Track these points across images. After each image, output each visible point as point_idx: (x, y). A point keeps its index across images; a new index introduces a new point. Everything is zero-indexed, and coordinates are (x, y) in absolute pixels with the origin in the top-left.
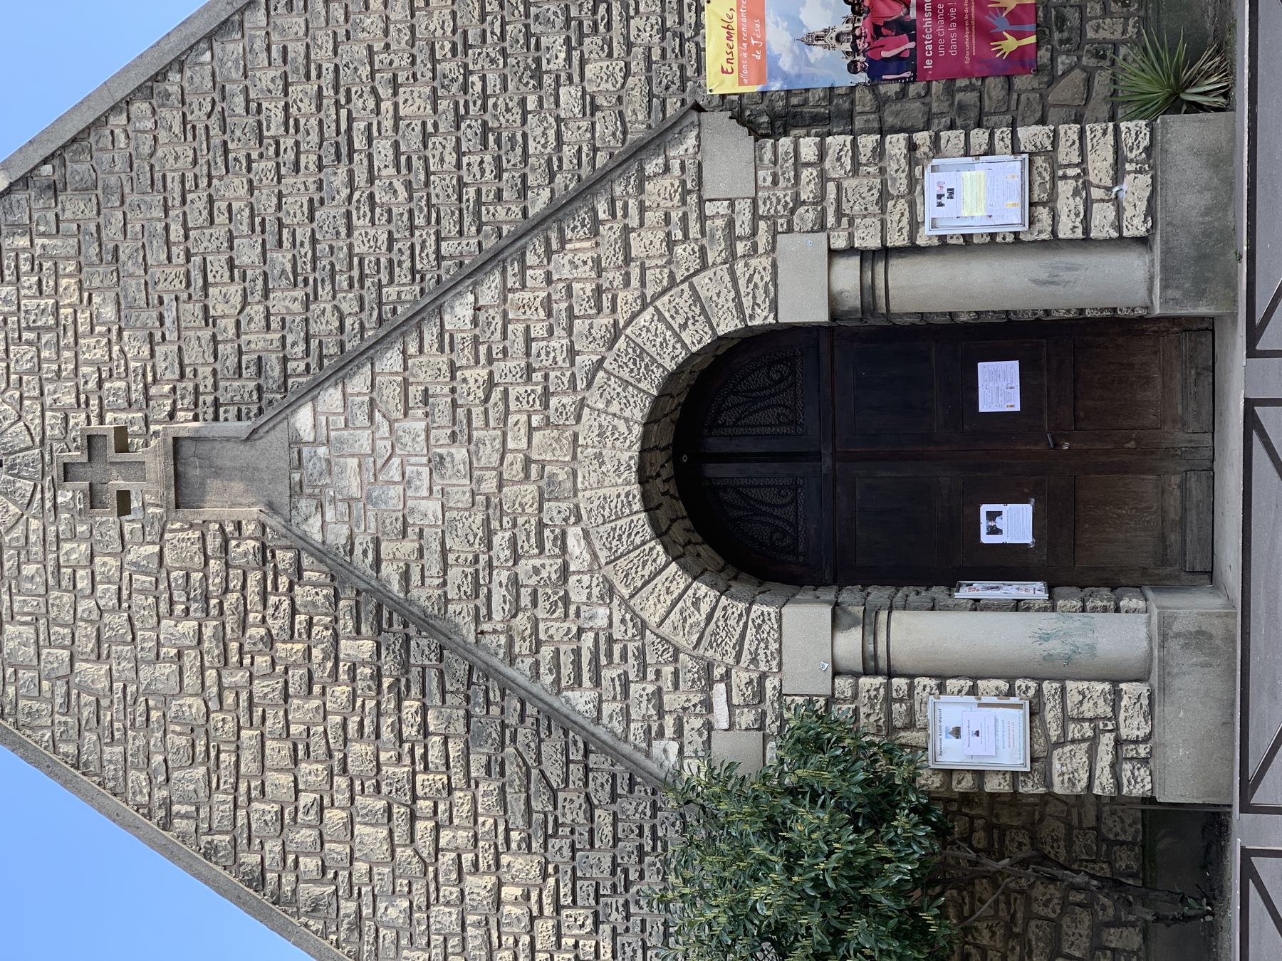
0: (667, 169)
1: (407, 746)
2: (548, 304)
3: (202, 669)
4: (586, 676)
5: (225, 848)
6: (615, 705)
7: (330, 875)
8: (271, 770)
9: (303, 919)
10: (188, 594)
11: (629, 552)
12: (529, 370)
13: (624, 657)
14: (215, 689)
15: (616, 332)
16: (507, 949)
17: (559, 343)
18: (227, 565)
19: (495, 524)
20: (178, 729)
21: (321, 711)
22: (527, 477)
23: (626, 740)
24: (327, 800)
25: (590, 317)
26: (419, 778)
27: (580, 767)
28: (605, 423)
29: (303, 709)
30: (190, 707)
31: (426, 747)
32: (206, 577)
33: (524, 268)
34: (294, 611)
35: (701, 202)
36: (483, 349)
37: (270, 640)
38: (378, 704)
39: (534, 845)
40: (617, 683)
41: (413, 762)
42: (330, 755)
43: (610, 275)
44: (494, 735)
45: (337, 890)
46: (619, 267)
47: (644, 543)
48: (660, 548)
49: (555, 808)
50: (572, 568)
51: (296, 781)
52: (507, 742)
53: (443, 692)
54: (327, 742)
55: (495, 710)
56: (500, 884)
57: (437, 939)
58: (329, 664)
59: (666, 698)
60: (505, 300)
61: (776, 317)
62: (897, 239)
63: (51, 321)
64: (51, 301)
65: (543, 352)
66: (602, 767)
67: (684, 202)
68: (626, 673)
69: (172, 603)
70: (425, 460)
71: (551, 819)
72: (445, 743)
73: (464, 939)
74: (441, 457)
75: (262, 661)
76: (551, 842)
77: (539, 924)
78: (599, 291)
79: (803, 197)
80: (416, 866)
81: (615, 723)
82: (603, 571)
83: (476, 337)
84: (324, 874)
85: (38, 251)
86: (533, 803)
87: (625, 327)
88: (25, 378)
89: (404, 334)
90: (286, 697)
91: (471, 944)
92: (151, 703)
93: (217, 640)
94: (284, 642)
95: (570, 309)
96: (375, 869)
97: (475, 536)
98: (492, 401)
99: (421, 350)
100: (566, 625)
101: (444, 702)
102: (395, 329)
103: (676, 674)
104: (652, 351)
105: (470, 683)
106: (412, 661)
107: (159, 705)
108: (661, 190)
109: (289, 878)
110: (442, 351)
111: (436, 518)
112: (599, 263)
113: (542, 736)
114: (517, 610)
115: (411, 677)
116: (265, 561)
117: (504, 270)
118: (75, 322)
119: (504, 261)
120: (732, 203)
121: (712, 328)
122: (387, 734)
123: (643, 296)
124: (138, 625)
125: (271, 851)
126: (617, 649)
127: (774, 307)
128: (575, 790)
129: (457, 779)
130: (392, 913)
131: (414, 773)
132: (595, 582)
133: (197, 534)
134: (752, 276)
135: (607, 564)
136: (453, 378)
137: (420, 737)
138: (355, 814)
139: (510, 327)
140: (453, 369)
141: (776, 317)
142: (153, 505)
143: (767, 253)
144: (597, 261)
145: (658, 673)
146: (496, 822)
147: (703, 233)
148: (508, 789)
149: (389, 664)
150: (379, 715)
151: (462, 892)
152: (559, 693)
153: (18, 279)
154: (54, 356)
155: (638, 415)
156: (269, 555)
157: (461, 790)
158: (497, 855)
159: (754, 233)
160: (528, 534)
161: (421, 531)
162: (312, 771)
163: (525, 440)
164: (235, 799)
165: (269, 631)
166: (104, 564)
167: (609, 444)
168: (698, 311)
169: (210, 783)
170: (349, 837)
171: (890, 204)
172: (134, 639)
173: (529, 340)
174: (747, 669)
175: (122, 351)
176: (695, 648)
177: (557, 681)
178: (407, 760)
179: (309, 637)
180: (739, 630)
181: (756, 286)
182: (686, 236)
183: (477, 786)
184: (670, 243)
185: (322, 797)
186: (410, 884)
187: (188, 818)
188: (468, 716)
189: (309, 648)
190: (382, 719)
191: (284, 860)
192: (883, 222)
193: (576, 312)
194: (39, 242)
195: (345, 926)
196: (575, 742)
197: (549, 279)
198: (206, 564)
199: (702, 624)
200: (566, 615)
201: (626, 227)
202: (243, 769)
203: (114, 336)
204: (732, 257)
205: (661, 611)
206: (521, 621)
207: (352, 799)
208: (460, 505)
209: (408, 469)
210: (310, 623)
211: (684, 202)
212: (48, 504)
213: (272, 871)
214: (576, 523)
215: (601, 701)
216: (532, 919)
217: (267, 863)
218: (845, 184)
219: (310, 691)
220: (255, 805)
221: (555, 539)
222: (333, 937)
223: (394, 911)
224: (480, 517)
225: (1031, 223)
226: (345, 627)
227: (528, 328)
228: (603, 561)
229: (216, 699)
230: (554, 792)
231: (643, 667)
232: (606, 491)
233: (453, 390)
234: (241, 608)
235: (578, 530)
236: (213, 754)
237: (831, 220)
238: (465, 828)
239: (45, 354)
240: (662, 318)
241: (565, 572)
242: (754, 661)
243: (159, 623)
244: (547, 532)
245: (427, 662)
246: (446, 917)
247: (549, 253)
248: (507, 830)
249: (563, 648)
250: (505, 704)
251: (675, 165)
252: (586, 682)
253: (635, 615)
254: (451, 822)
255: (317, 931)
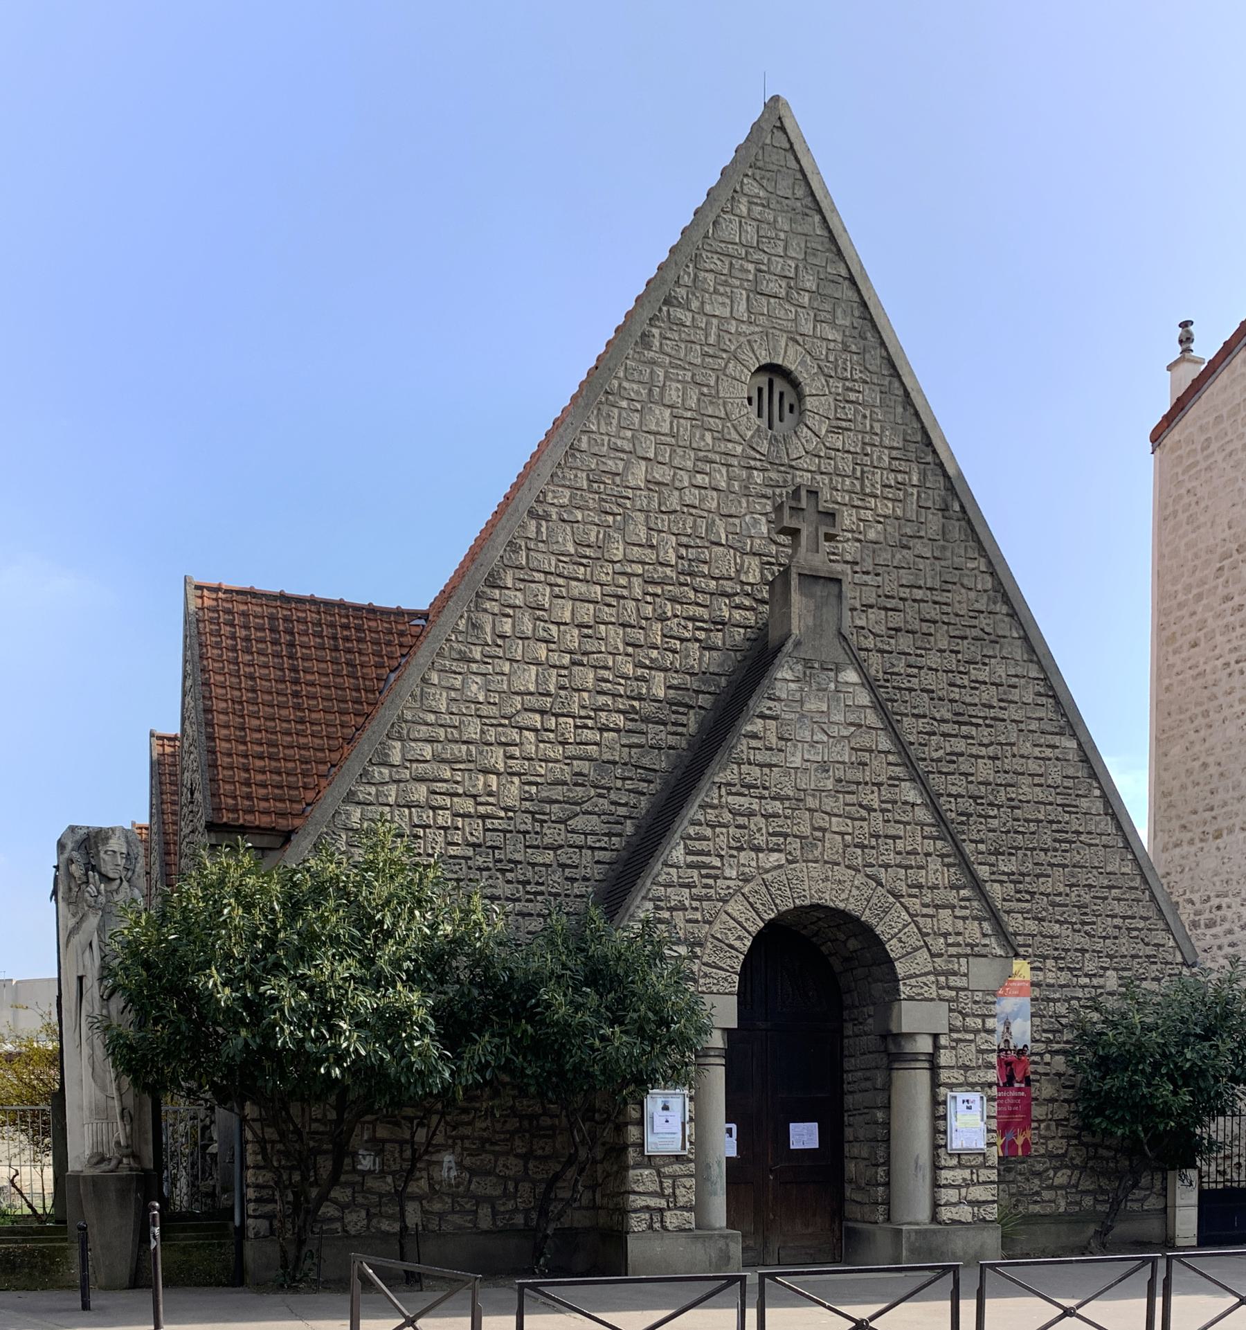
0: (985, 935)
1: (592, 714)
2: (914, 853)
3: (643, 563)
4: (695, 858)
5: (517, 559)
6: (675, 877)
7: (500, 642)
8: (573, 605)
9: (466, 615)
10: (693, 561)
11: (770, 895)
12: (877, 837)
13: (707, 886)
14: (629, 570)
15: (897, 896)
16: (452, 775)
17: (891, 858)
18: (712, 594)
19: (787, 804)
20: (601, 536)
21: (615, 651)
22: (815, 829)
23: (653, 883)
24: (553, 646)
25: (907, 879)
26: (570, 721)
27: (583, 843)
28: (846, 884)
29: (615, 636)
30: (617, 549)
31: (592, 728)
32: (704, 576)
33: (935, 838)
34: (682, 640)
35: (966, 956)
36: (889, 806)
37: (662, 619)
38: (621, 696)
39: (527, 803)
40: (691, 880)
41: (581, 717)
42: (585, 654)
43: (929, 895)
44: (603, 781)
45: (488, 645)
46: (933, 901)
47: (776, 905)
48: (773, 916)
49: (553, 822)
50: (761, 855)
51: (565, 624)
52: (598, 791)
53: (630, 746)
54: (594, 653)
55: (619, 783)
56: (498, 774)
57: (456, 720)
58: (647, 662)
59: (681, 913)
60: (916, 824)
61: (905, 999)
62: (944, 1076)
63: (868, 491)
64: (879, 492)
65: (887, 847)
66: (583, 859)
67: (967, 945)
68: (695, 887)
69: (687, 547)
70: (826, 759)
71: (546, 817)
72: (595, 744)
73: (457, 742)
74: (828, 771)
75: (648, 611)
76: (529, 816)
77: (471, 801)
78: (920, 887)
79: (967, 1019)
80: (509, 711)
81: (664, 877)
82: (758, 876)
83: (896, 802)
84: (499, 636)
85: (910, 490)
86: (556, 805)
87: (900, 902)
88: (832, 462)
89: (899, 753)
90: (624, 625)
91: (455, 747)
92: (619, 518)
93: (663, 578)
94: (662, 630)
95: (911, 867)
96: (505, 678)
97: (781, 789)
98: (860, 810)
99: (889, 764)
100: (725, 847)
101: (623, 746)
102: (903, 747)
103: (697, 921)
104: (887, 919)
105: (637, 767)
106: (650, 725)
107: (617, 524)
108: (973, 931)
109: (494, 607)
110: (889, 779)
111: (791, 763)
112: (935, 888)
113: (603, 817)
114: (734, 813)
115: (639, 723)
116: (715, 623)
117: (933, 826)
118: (867, 509)
119: (938, 826)
120: (966, 975)
121: (899, 958)
122: (601, 700)
123: (917, 915)
124: (672, 517)
125: (515, 596)
126: (711, 881)
127: (910, 999)
128: (566, 837)
129: (571, 751)
130: (474, 688)
131: (574, 717)
132: (752, 870)
133: (733, 575)
134: (927, 985)
135: (763, 879)
136: (874, 784)
137: (599, 725)
138: (543, 667)
139: (902, 826)
140: (879, 785)
141: (905, 999)
142: (752, 544)
143: (938, 995)
144: (936, 887)
145: (696, 909)
146: (542, 776)
147: (950, 956)
148: (565, 787)
149: (648, 708)
150: (614, 695)
151: (491, 744)
152: (682, 838)
153: (893, 471)
154: (846, 488)
155: (851, 907)
156: (720, 627)
157: (564, 752)
158: (519, 774)
159: (950, 988)
160: (781, 826)
161: (782, 751)
162: (572, 638)
163: (837, 830)
164: (551, 574)
165: (669, 619)
166: (713, 499)
167: (834, 886)
168: (909, 950)
169: (563, 555)
170: (528, 660)
171: (962, 1072)
172: (662, 512)
173: (894, 838)
174: (700, 970)
175: (848, 540)
176: (712, 935)
177: (690, 838)
178: (583, 713)
179: (665, 649)
180: (724, 966)
181: (922, 988)
182: (949, 945)
183: (566, 764)
184: (945, 935)
185: (554, 643)
186: (495, 704)
187: (537, 533)
188: (614, 763)
189: (658, 648)
190: (610, 697)
191: (509, 606)
192: (952, 1067)
193: (909, 871)
194: (915, 491)
195: (463, 648)
196: (599, 841)
197: (928, 854)
198: (713, 578)
199: (727, 941)
200: (731, 848)
201: (955, 907)
202: (574, 583)
203: (856, 535)
204: (936, 973)
205: (735, 914)
206: (727, 817)
207: (554, 667)
208: (798, 780)
209: (820, 746)
210: (674, 652)
211: (967, 945)
212: (752, 463)
213: (500, 594)
214: (787, 859)
215: (678, 867)
216: (474, 797)
217: (507, 592)
218: (973, 1045)
219: (628, 644)
220: (548, 589)
221: (779, 845)
222: (453, 638)
223: (475, 689)
224: (791, 794)
225: (950, 1155)
226: (673, 678)
227: (901, 838)
228: (765, 876)
229: (622, 570)
230: (563, 822)
231: (700, 899)
232: (806, 883)
233: (866, 783)
234: (684, 600)
235: (783, 862)
236: (584, 561)
237: (955, 1036)
238: (537, 751)
239: (848, 481)
240: (905, 926)
241: (757, 849)
242: (706, 975)
243: (674, 534)
244: (782, 839)
245: (650, 736)
246: (473, 730)
247: (942, 856)
248: (537, 784)
249: (711, 843)
250: (623, 792)
251: (986, 941)
252: (690, 858)
253: (732, 895)
254: (541, 741)
255: (458, 625)
